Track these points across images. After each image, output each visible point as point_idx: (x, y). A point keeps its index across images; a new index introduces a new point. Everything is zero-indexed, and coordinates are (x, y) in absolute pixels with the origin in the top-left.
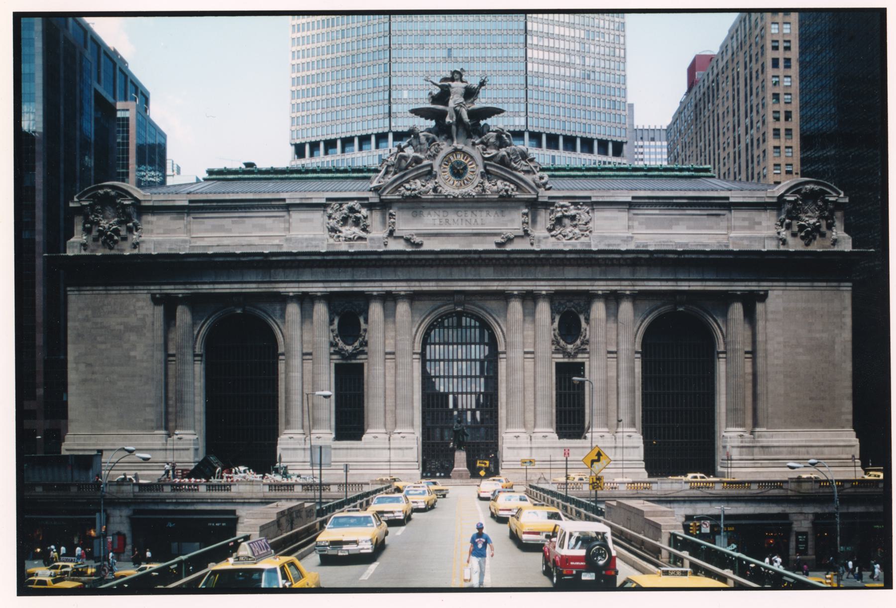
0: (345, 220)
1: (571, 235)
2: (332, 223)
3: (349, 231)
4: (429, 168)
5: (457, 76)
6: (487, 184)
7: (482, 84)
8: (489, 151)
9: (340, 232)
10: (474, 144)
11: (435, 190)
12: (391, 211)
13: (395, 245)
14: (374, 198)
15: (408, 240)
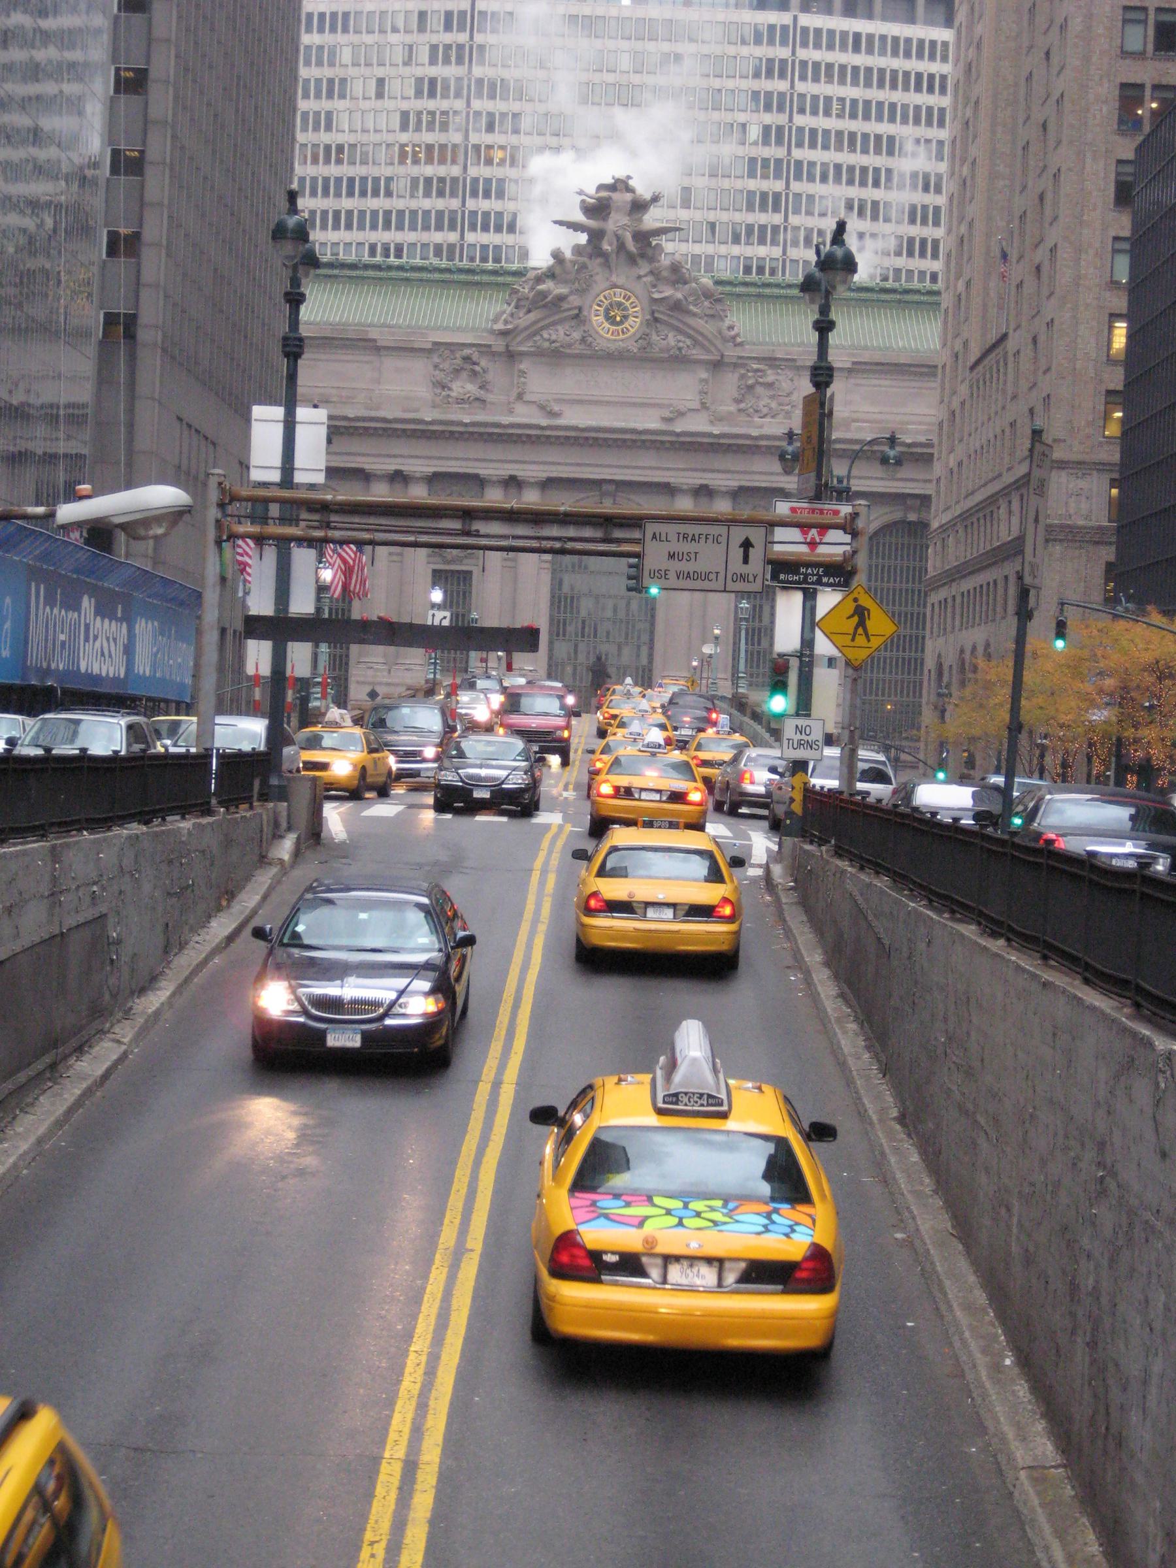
0: (457, 371)
1: (765, 410)
2: (440, 375)
3: (463, 387)
4: (576, 311)
5: (619, 186)
6: (654, 337)
7: (655, 199)
8: (661, 287)
9: (450, 389)
10: (639, 277)
11: (583, 340)
12: (522, 367)
13: (524, 415)
14: (499, 345)
15: (542, 408)
